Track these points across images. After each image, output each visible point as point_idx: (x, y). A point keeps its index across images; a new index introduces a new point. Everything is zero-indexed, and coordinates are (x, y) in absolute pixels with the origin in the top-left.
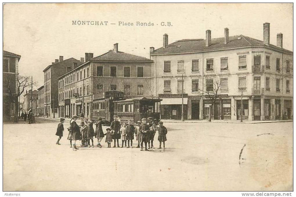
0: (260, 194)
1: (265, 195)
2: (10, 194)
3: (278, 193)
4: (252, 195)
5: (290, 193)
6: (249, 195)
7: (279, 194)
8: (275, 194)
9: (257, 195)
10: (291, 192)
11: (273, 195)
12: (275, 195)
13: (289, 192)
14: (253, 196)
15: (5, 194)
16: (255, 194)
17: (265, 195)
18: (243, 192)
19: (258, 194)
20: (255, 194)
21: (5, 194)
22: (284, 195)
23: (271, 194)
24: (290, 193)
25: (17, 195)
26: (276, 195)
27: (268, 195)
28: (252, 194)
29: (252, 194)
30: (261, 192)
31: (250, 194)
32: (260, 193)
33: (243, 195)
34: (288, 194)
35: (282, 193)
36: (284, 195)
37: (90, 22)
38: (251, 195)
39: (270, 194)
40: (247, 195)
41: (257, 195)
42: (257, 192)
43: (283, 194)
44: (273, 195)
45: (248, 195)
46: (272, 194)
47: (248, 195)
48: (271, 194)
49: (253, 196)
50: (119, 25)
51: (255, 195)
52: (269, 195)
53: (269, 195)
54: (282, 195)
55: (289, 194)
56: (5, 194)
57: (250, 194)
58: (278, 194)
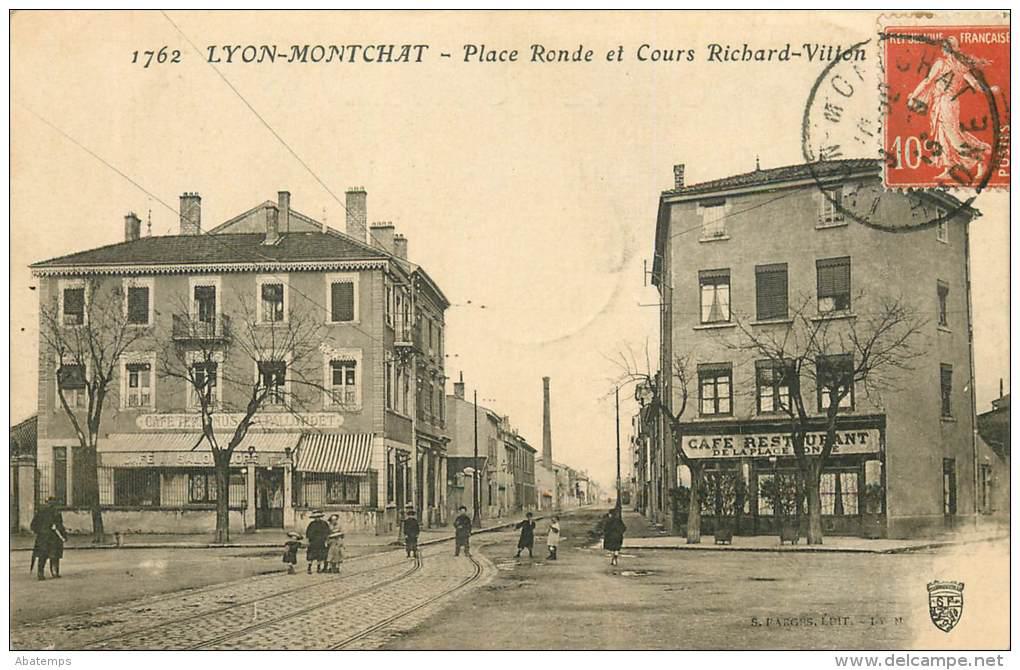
1: (915, 661)
2: (33, 662)
3: (957, 655)
4: (873, 662)
5: (999, 658)
6: (860, 665)
7: (962, 661)
11: (941, 661)
13: (994, 655)
14: (874, 665)
15: (19, 658)
17: (915, 661)
18: (840, 654)
21: (18, 661)
22: (979, 662)
23: (935, 661)
24: (999, 658)
25: (60, 663)
26: (951, 662)
27: (926, 662)
28: (872, 659)
29: (872, 659)
30: (903, 654)
31: (864, 661)
32: (898, 654)
34: (990, 661)
35: (970, 656)
36: (979, 662)
37: (364, 48)
38: (868, 665)
39: (932, 659)
40: (854, 665)
41: (890, 662)
42: (889, 654)
43: (976, 659)
44: (941, 661)
45: (856, 664)
47: (857, 662)
48: (935, 661)
49: (874, 665)
50: (466, 60)
51: (883, 663)
52: (928, 664)
53: (928, 664)
54: (973, 664)
55: (997, 660)
56: (18, 661)
57: (864, 661)
58: (959, 661)
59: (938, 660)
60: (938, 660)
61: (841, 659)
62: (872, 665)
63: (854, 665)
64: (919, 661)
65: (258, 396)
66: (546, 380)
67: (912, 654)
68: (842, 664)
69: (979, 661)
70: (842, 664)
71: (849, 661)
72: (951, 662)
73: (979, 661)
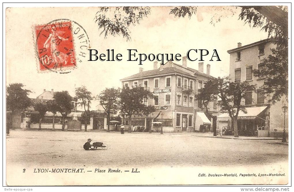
1: (264, 190)
3: (276, 188)
4: (252, 190)
5: (288, 188)
6: (248, 191)
7: (277, 190)
8: (257, 190)
10: (289, 187)
11: (271, 190)
13: (287, 188)
14: (252, 191)
16: (254, 189)
17: (264, 190)
20: (254, 189)
22: (282, 190)
23: (270, 189)
24: (288, 188)
26: (274, 190)
27: (267, 190)
28: (243, 189)
30: (260, 188)
31: (249, 189)
32: (259, 188)
34: (285, 189)
35: (280, 188)
36: (282, 190)
38: (250, 191)
40: (246, 191)
41: (256, 190)
42: (256, 187)
44: (271, 190)
46: (270, 189)
47: (247, 190)
48: (270, 189)
49: (252, 191)
51: (255, 190)
52: (267, 190)
53: (267, 190)
57: (249, 189)
58: (277, 189)
61: (243, 189)
62: (251, 190)
63: (246, 191)
64: (265, 190)
67: (263, 188)
68: (243, 190)
69: (282, 190)
70: (243, 190)
71: (245, 189)
72: (274, 190)
73: (282, 190)
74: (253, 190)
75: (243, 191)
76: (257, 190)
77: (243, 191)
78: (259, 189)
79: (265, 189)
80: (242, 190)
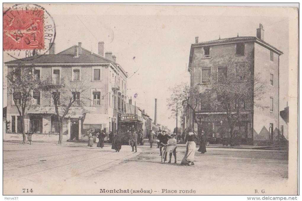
0: (266, 198)
1: (271, 199)
3: (283, 197)
4: (258, 199)
5: (296, 197)
7: (285, 199)
8: (264, 199)
9: (263, 198)
10: (297, 196)
11: (279, 198)
12: (281, 199)
13: (294, 196)
14: (259, 199)
16: (261, 198)
17: (271, 199)
19: (264, 198)
20: (261, 198)
22: (290, 199)
23: (277, 198)
24: (296, 197)
26: (282, 198)
27: (274, 199)
28: (249, 198)
30: (268, 196)
31: (256, 198)
32: (266, 196)
33: (248, 199)
34: (293, 198)
35: (287, 197)
36: (290, 199)
41: (263, 198)
42: (263, 196)
43: (289, 198)
44: (279, 198)
47: (254, 199)
48: (277, 198)
49: (259, 199)
55: (295, 198)
57: (256, 198)
59: (278, 198)
60: (278, 198)
61: (249, 198)
63: (253, 199)
65: (72, 102)
66: (156, 100)
67: (270, 196)
68: (249, 199)
70: (249, 199)
72: (282, 198)
74: (260, 199)
75: (250, 199)
76: (264, 199)
77: (250, 199)
78: (266, 198)
79: (273, 198)
80: (249, 199)
